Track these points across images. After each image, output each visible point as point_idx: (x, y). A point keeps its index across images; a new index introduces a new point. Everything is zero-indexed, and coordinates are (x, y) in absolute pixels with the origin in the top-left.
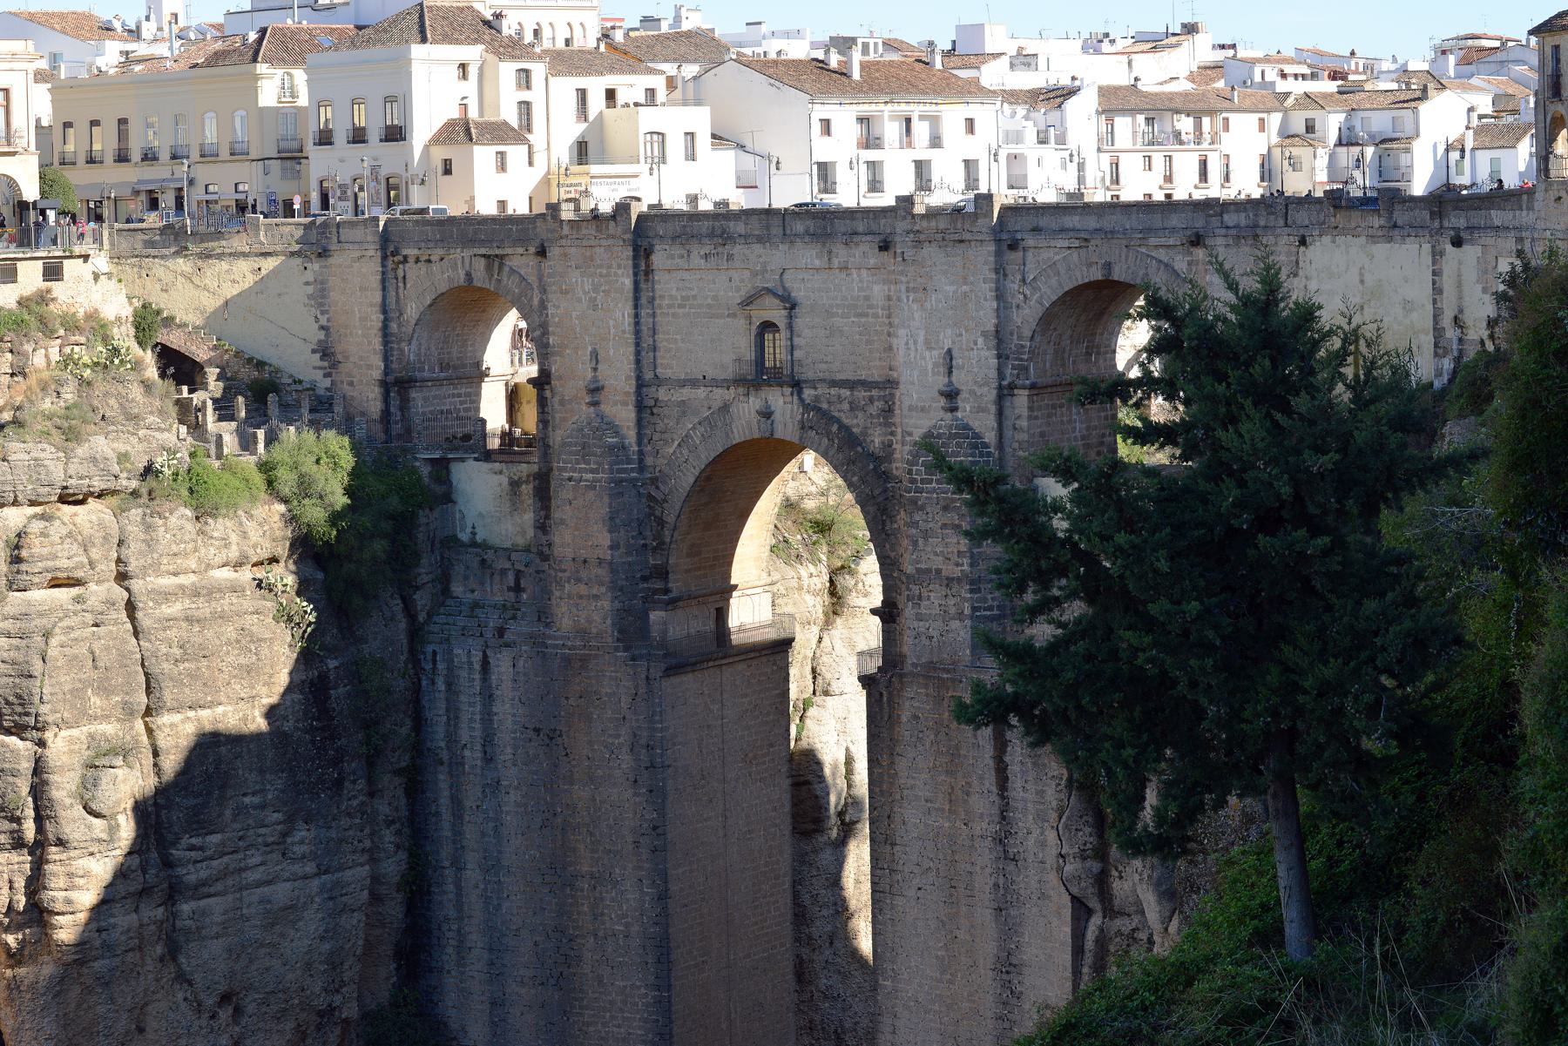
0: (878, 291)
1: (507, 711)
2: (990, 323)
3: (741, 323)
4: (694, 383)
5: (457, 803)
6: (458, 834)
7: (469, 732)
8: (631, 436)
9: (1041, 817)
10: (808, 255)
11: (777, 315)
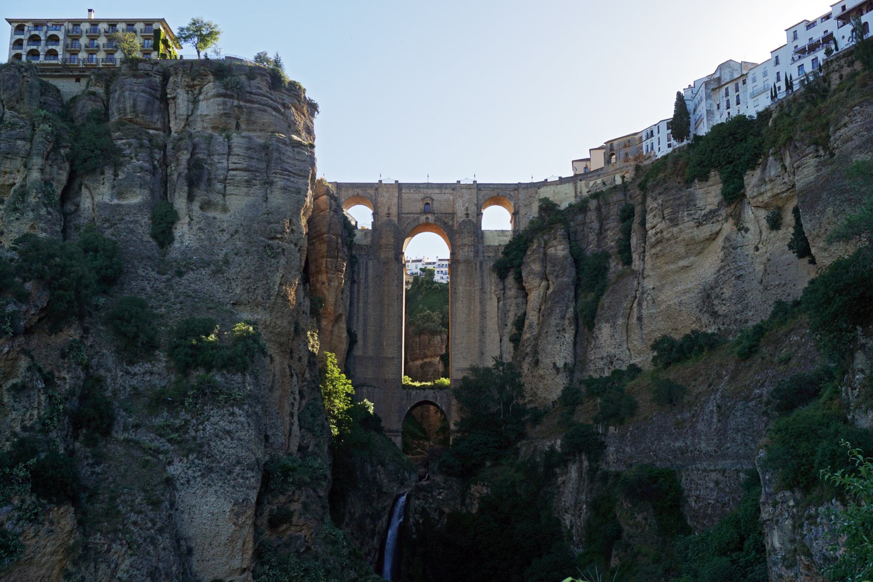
0: (451, 198)
1: (371, 272)
2: (476, 202)
3: (421, 203)
4: (410, 214)
5: (358, 290)
6: (358, 296)
7: (362, 276)
8: (397, 223)
9: (491, 285)
10: (437, 191)
11: (430, 202)
